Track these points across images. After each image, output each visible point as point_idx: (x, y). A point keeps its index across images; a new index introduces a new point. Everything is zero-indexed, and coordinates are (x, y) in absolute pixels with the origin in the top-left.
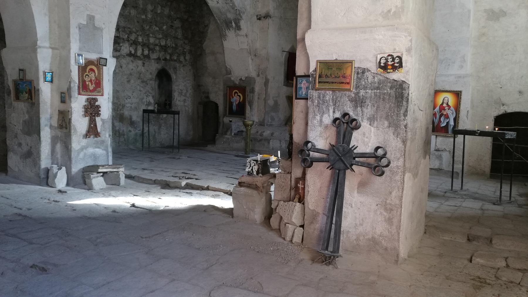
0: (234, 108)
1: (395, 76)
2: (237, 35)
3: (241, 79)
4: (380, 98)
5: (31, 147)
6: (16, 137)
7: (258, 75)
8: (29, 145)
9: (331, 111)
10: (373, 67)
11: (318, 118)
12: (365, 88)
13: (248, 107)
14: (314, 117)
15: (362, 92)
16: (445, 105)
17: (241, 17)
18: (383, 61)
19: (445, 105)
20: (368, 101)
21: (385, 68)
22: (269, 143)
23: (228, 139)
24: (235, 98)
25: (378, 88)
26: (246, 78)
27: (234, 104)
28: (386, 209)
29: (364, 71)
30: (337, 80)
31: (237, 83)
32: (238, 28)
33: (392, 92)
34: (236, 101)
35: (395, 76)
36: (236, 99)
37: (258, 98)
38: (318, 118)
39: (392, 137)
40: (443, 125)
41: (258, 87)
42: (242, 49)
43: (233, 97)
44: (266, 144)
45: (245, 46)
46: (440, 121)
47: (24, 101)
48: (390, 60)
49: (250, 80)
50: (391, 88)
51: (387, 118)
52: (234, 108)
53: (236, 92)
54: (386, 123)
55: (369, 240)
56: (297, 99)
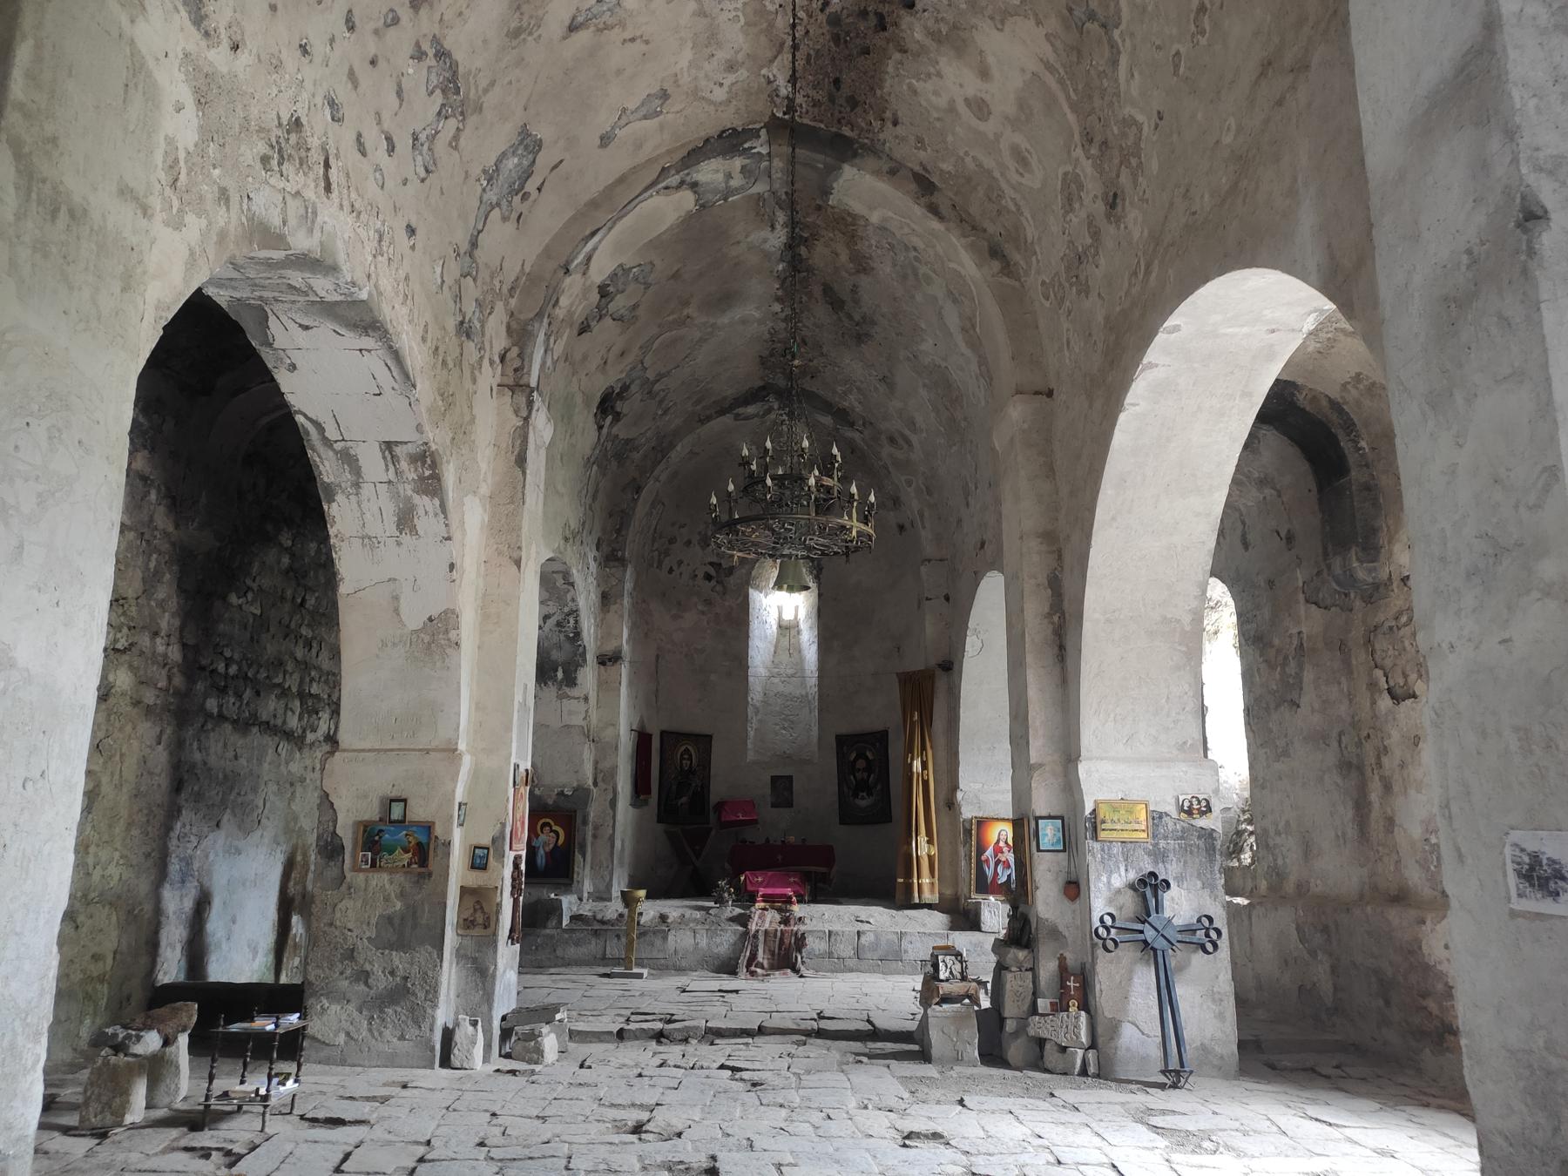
0: (541, 860)
1: (1202, 822)
2: (560, 697)
3: (561, 793)
4: (1186, 850)
5: (406, 978)
6: (351, 954)
7: (595, 784)
8: (401, 973)
9: (1122, 869)
10: (1172, 809)
11: (1104, 879)
12: (1166, 838)
13: (578, 857)
14: (1099, 879)
15: (1162, 843)
16: (1002, 844)
17: (585, 660)
18: (1186, 804)
19: (1002, 844)
20: (1171, 855)
21: (1189, 812)
22: (665, 938)
23: (552, 937)
24: (543, 837)
25: (1182, 838)
26: (575, 790)
27: (541, 852)
28: (1214, 1001)
29: (1161, 815)
30: (1128, 827)
31: (550, 802)
32: (571, 681)
33: (1201, 843)
34: (545, 844)
35: (1202, 822)
36: (546, 840)
37: (595, 836)
38: (1104, 879)
39: (1208, 901)
40: (1004, 879)
41: (593, 812)
42: (567, 726)
43: (537, 836)
44: (658, 942)
45: (577, 720)
46: (996, 873)
47: (392, 871)
48: (1195, 802)
49: (582, 794)
50: (1199, 838)
51: (1199, 876)
52: (541, 860)
53: (548, 824)
54: (1199, 884)
55: (1197, 1048)
56: (1039, 850)
